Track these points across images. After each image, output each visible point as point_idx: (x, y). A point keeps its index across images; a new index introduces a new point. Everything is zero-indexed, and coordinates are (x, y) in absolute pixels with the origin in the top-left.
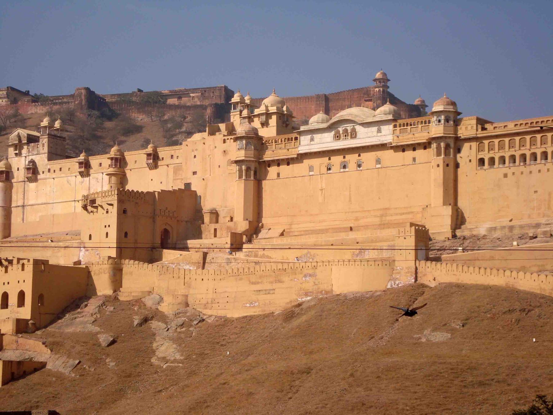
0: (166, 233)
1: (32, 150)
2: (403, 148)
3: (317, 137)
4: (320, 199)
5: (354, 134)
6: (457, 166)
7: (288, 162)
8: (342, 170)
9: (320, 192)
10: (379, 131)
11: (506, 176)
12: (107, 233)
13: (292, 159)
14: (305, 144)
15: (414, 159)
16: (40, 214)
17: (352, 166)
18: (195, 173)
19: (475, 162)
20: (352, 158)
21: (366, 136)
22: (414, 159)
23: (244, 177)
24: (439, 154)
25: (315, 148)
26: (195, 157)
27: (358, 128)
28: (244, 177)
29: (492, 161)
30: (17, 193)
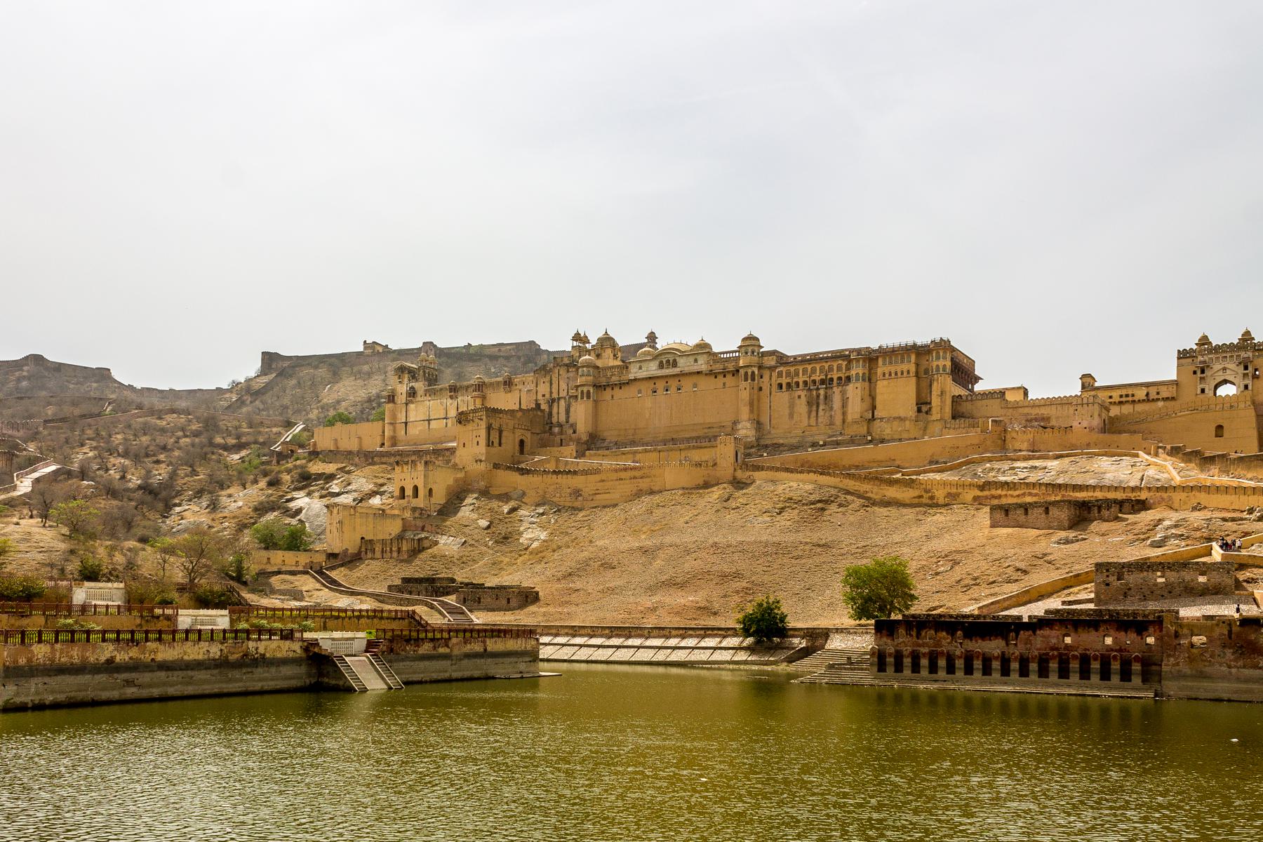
0: (522, 442)
3: (644, 365)
5: (675, 364)
6: (761, 389)
7: (621, 385)
14: (634, 372)
19: (775, 387)
20: (673, 384)
21: (684, 365)
24: (746, 380)
25: (643, 374)
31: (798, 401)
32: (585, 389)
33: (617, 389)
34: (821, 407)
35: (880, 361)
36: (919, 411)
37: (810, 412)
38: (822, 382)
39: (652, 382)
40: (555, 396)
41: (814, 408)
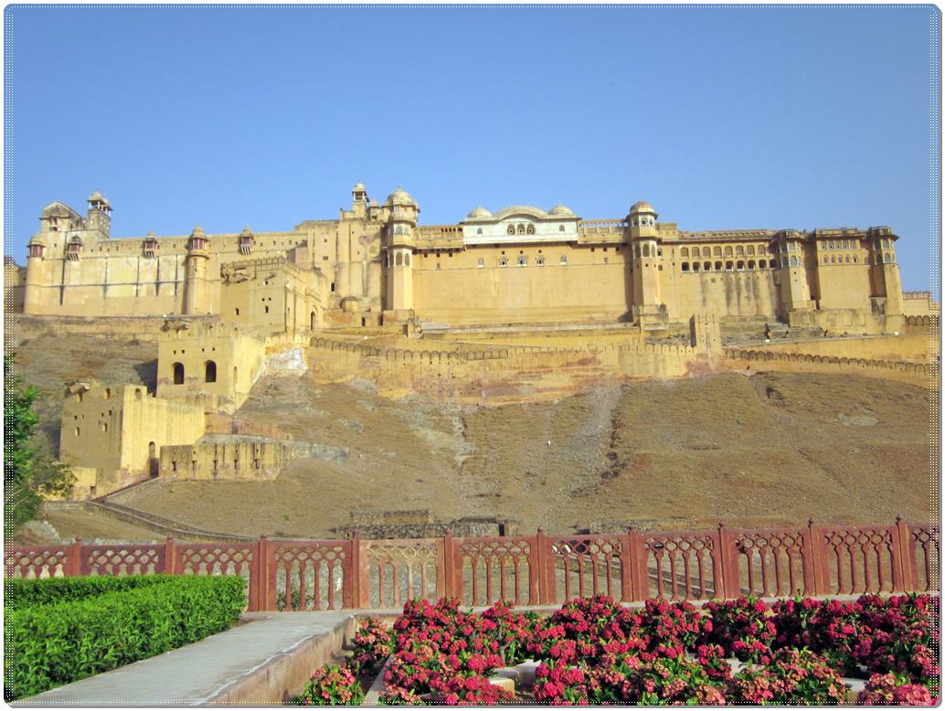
1: (77, 225)
2: (593, 247)
4: (494, 294)
5: (531, 231)
7: (450, 252)
8: (519, 265)
9: (493, 287)
10: (562, 229)
11: (713, 280)
12: (267, 308)
13: (458, 250)
14: (470, 235)
15: (606, 259)
16: (87, 296)
17: (532, 262)
18: (326, 258)
20: (532, 253)
21: (545, 232)
22: (606, 259)
23: (404, 264)
26: (326, 241)
27: (537, 226)
28: (404, 264)
29: (707, 266)
30: (53, 272)
31: (712, 286)
32: (405, 251)
33: (444, 256)
34: (744, 294)
35: (819, 244)
36: (874, 305)
37: (728, 299)
38: (740, 265)
39: (501, 250)
40: (344, 258)
41: (734, 295)
